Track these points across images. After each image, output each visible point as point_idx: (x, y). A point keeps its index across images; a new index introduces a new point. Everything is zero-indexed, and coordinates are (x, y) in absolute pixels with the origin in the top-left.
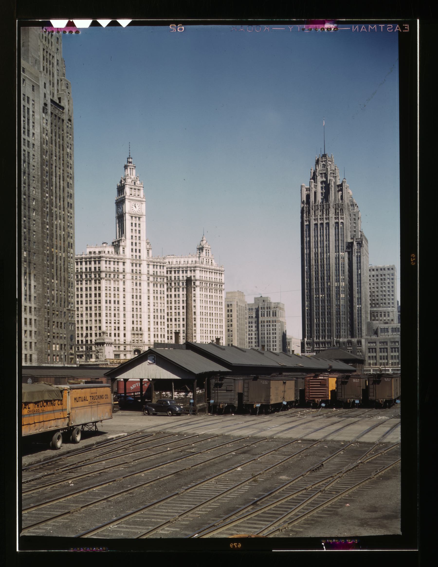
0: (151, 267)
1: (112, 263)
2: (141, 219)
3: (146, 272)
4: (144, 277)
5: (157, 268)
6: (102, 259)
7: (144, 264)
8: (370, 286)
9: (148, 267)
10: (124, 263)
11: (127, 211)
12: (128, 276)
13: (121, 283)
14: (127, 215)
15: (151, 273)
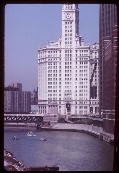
0: (78, 52)
1: (53, 52)
2: (72, 22)
3: (75, 56)
4: (74, 59)
5: (82, 52)
6: (47, 50)
7: (74, 51)
8: (65, 69)
9: (76, 52)
10: (60, 51)
11: (63, 19)
12: (63, 59)
13: (58, 63)
14: (63, 22)
15: (78, 55)
